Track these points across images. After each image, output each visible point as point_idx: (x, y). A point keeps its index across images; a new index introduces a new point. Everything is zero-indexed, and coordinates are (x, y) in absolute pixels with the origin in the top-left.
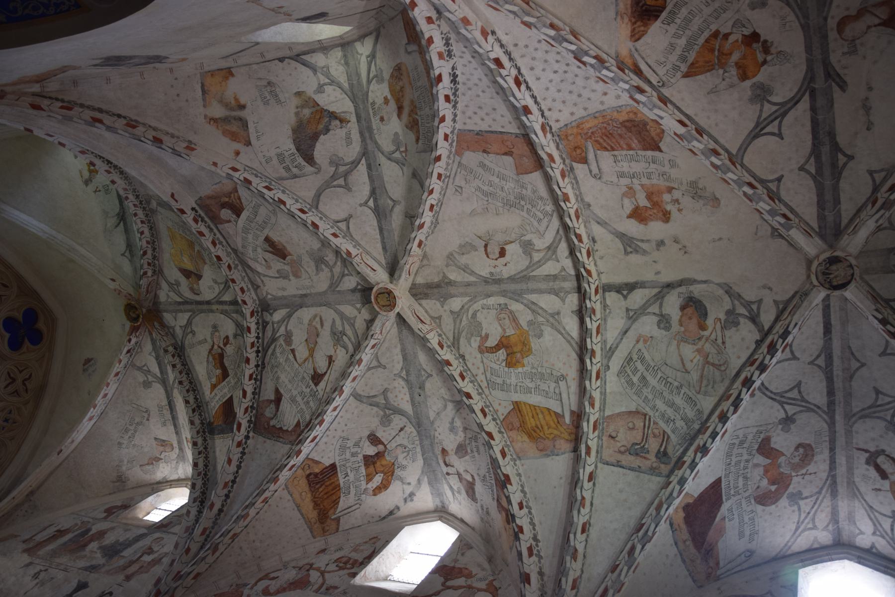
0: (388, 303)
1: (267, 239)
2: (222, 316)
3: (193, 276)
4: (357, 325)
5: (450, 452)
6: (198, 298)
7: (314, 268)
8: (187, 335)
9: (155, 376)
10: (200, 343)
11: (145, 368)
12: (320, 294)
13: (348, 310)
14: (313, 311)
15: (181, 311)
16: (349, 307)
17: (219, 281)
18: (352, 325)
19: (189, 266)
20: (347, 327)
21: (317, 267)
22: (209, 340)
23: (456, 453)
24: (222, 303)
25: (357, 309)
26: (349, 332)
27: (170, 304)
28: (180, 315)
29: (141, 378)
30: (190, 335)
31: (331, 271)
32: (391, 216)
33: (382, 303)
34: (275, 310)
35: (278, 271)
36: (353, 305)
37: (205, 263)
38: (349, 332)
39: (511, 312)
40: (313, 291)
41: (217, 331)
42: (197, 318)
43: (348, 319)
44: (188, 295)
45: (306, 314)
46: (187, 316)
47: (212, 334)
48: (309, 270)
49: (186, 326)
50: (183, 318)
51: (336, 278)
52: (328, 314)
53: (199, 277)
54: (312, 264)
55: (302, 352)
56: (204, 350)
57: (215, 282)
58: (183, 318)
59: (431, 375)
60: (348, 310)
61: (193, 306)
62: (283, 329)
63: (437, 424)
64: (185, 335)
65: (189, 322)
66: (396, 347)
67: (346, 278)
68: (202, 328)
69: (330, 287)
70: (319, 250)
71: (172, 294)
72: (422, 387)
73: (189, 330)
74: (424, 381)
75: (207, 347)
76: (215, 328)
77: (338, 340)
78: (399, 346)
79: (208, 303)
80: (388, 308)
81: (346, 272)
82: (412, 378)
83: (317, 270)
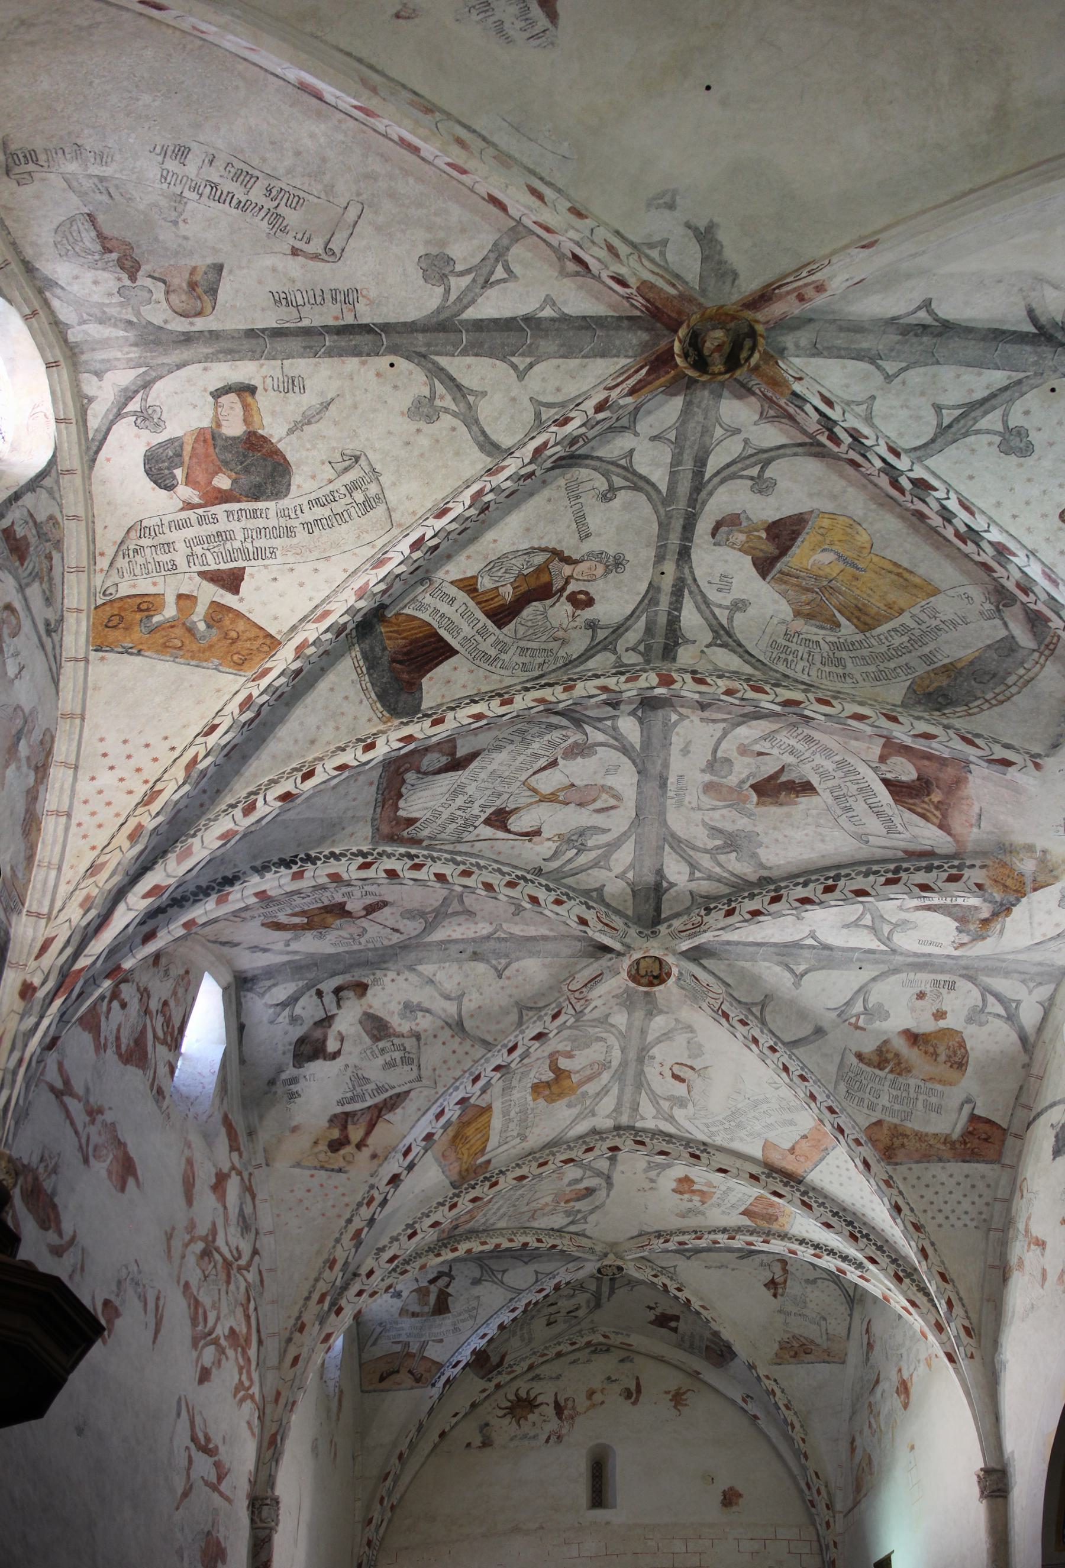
0: (642, 972)
1: (807, 788)
2: (643, 587)
3: (770, 549)
4: (595, 872)
5: (364, 1001)
6: (703, 527)
7: (719, 825)
8: (606, 475)
9: (467, 299)
10: (580, 519)
11: (500, 273)
12: (662, 813)
13: (624, 857)
14: (630, 794)
15: (676, 461)
16: (629, 859)
17: (739, 617)
18: (595, 864)
19: (806, 556)
20: (593, 855)
21: (721, 831)
22: (586, 547)
23: (366, 1014)
24: (678, 593)
25: (624, 872)
26: (583, 859)
27: (706, 431)
28: (665, 454)
29: (465, 251)
30: (601, 484)
31: (706, 851)
32: (780, 963)
33: (643, 963)
34: (641, 721)
35: (728, 761)
36: (632, 866)
37: (797, 614)
38: (583, 859)
39: (600, 1074)
40: (670, 803)
41: (607, 571)
42: (647, 510)
43: (607, 856)
44: (722, 501)
45: (625, 780)
46: (660, 477)
47: (599, 556)
48: (717, 814)
49: (629, 471)
50: (654, 463)
51: (691, 853)
52: (619, 821)
53: (764, 566)
54: (729, 827)
55: (548, 781)
56: (560, 535)
57: (739, 606)
58: (654, 463)
59: (500, 976)
60: (624, 857)
61: (682, 504)
62: (600, 737)
63: (413, 977)
64: (606, 467)
65: (639, 483)
66: (552, 930)
67: (687, 870)
68: (620, 525)
69: (673, 835)
70: (754, 855)
71: (732, 448)
72: (476, 956)
73: (618, 482)
74: (488, 962)
75: (570, 545)
76: (617, 563)
77: (569, 840)
78: (552, 934)
79: (684, 554)
80: (633, 972)
81: (698, 874)
82: (492, 944)
83: (713, 828)
